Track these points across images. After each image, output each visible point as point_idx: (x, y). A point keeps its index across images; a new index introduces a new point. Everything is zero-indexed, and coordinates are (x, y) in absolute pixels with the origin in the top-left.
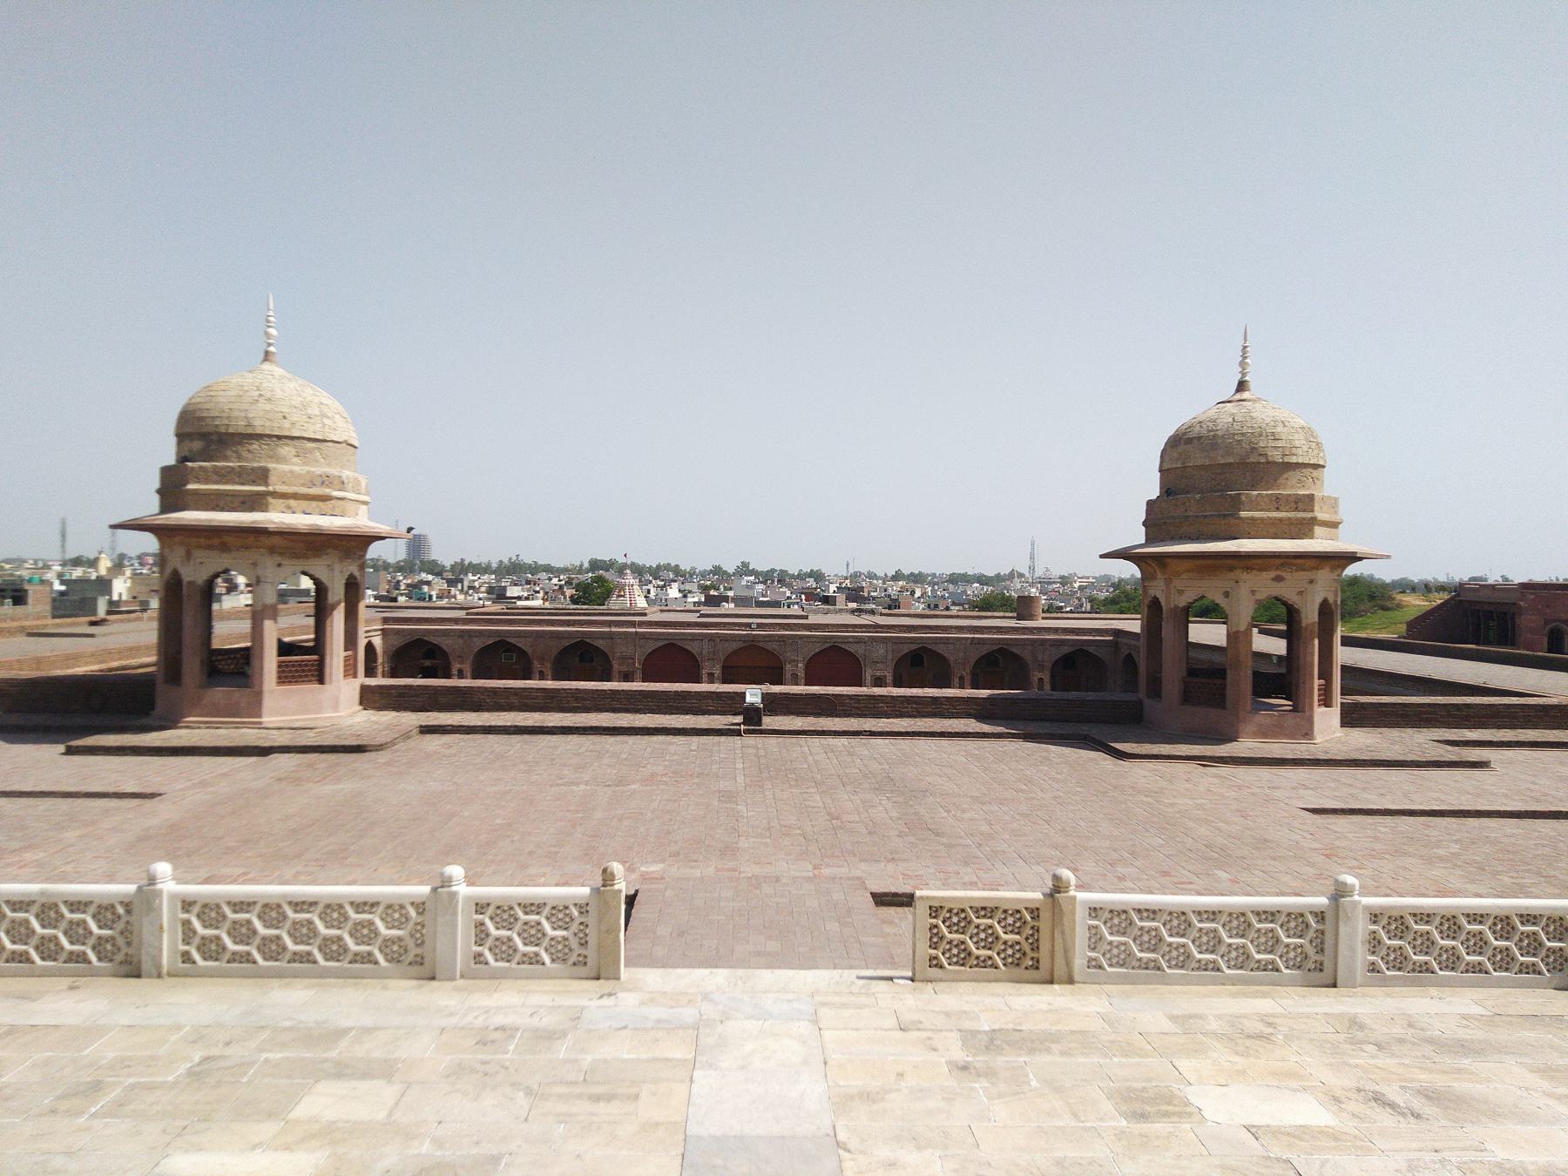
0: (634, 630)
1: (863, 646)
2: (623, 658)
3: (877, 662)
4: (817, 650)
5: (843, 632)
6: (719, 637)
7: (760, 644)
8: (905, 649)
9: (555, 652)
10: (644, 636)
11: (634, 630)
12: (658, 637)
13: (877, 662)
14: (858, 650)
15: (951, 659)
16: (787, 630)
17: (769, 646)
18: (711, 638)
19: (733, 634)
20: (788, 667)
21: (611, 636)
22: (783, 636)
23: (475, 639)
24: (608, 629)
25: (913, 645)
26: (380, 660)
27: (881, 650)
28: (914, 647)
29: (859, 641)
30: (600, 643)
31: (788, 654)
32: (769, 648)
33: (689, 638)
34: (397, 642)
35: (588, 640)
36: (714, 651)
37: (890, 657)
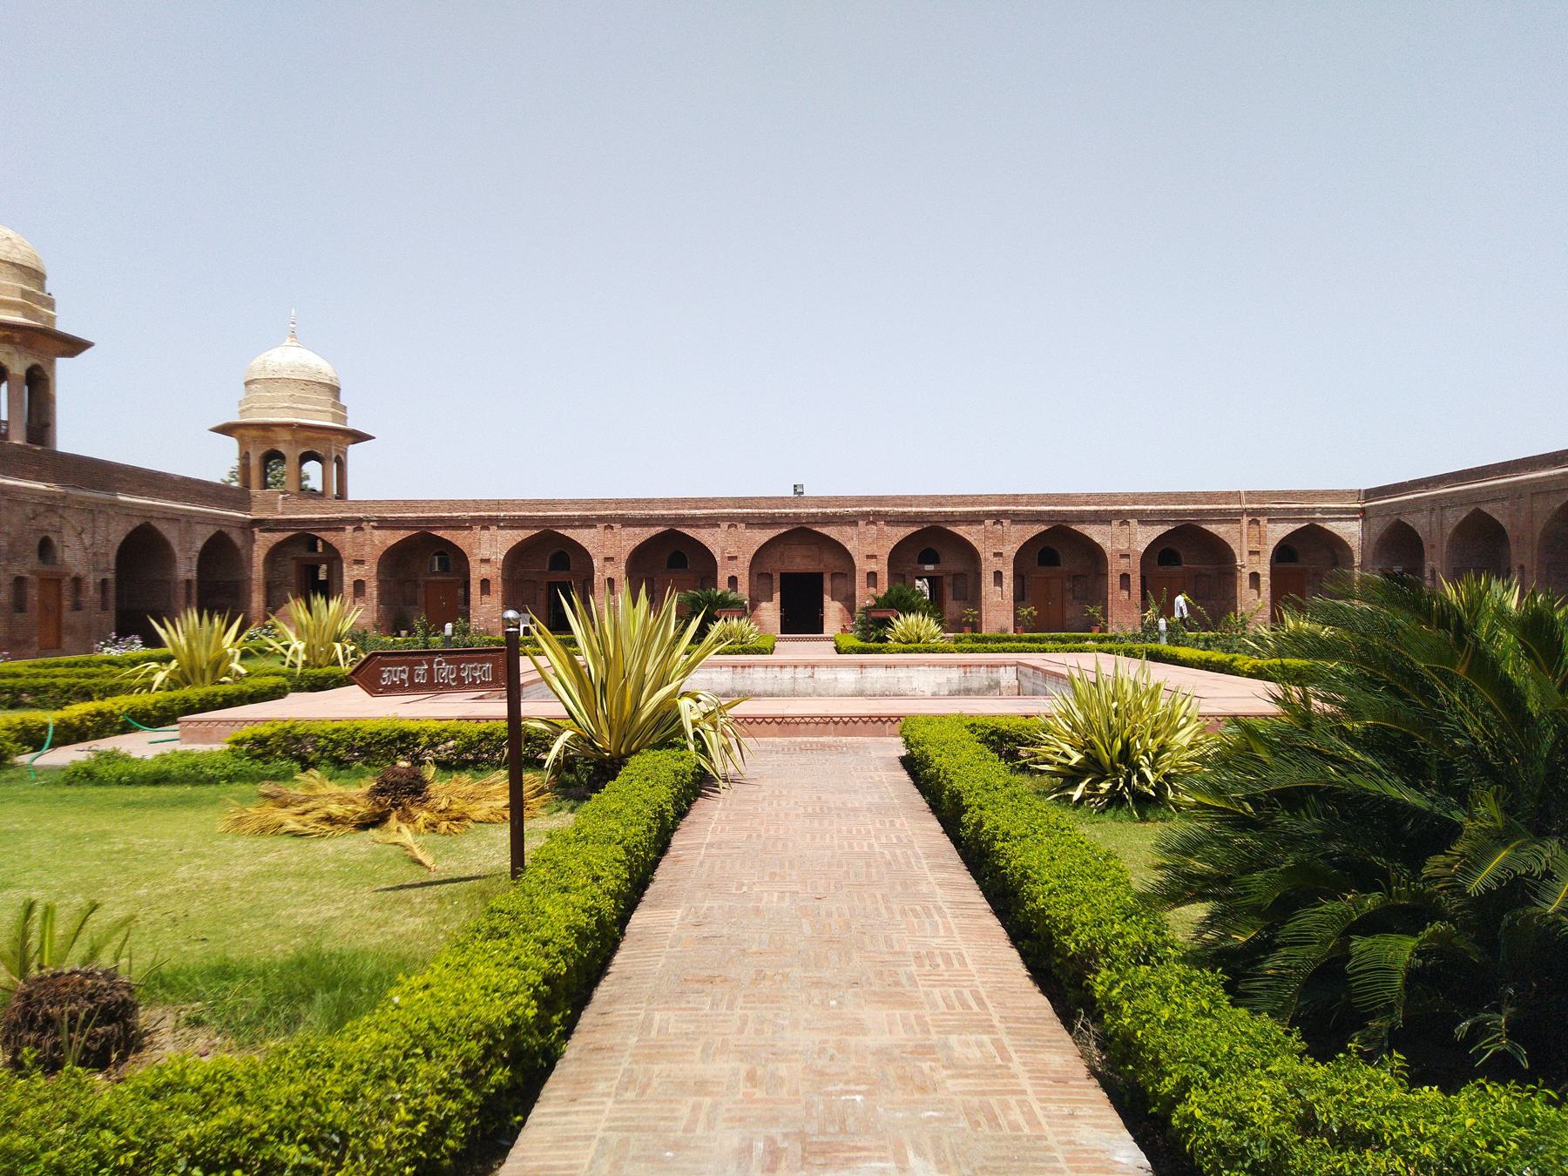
9: (1539, 525)
34: (1378, 526)
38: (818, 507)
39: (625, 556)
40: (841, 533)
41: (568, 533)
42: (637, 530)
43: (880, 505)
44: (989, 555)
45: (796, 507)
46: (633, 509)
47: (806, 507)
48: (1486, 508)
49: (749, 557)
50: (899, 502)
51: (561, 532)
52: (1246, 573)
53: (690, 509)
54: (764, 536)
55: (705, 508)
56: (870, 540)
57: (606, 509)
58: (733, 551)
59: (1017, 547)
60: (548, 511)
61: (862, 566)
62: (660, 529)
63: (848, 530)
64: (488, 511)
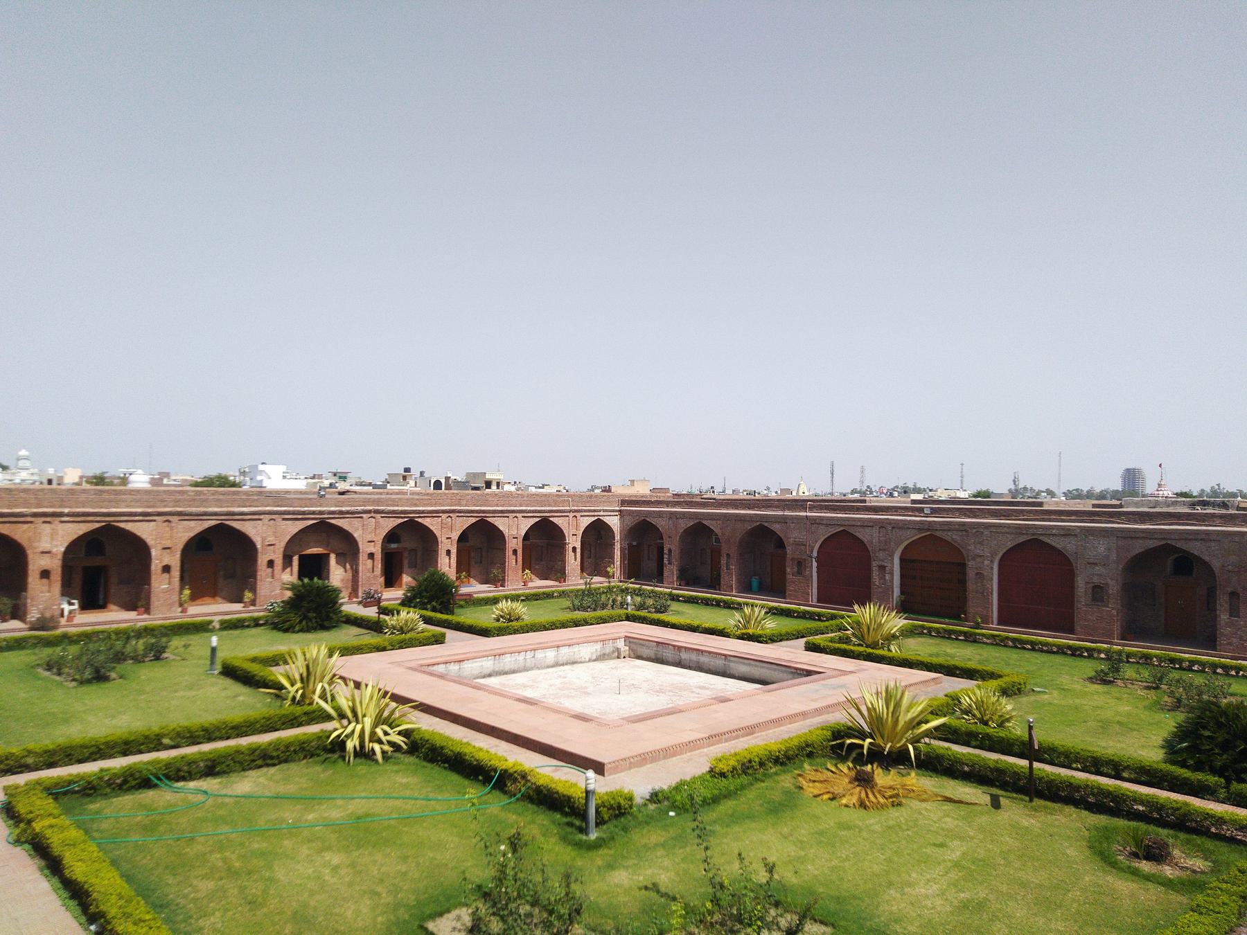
0: (804, 514)
1: (1073, 540)
2: (798, 544)
3: (1096, 564)
4: (1010, 545)
5: (1043, 520)
6: (890, 524)
7: (938, 534)
8: (1139, 547)
10: (814, 521)
11: (804, 514)
12: (829, 523)
13: (1096, 564)
14: (1068, 546)
15: (1216, 564)
16: (969, 517)
17: (948, 536)
18: (882, 525)
19: (906, 520)
20: (970, 564)
21: (784, 520)
22: (964, 524)
23: (680, 521)
24: (780, 513)
25: (1151, 542)
26: (617, 537)
27: (1101, 547)
28: (1152, 544)
29: (1067, 533)
30: (776, 527)
31: (972, 547)
32: (949, 540)
33: (859, 524)
35: (766, 524)
36: (886, 541)
37: (1114, 556)
38: (336, 506)
39: (180, 546)
40: (350, 524)
41: (129, 527)
42: (192, 524)
43: (378, 506)
44: (444, 539)
45: (320, 506)
46: (190, 506)
47: (327, 506)
48: (705, 522)
49: (283, 544)
50: (390, 503)
51: (122, 525)
52: (571, 546)
53: (239, 506)
54: (295, 527)
55: (250, 506)
56: (370, 530)
57: (165, 506)
58: (271, 540)
59: (459, 533)
60: (112, 507)
61: (365, 548)
62: (213, 523)
63: (356, 522)
64: (51, 507)
